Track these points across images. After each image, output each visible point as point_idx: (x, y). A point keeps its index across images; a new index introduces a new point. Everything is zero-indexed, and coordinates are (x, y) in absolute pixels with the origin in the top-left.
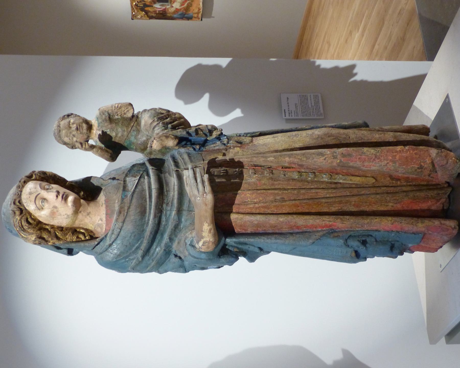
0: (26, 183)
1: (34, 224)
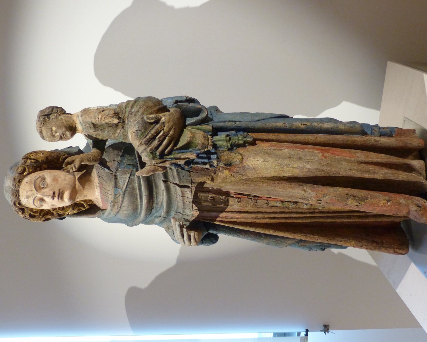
0: (21, 181)
1: (37, 215)
